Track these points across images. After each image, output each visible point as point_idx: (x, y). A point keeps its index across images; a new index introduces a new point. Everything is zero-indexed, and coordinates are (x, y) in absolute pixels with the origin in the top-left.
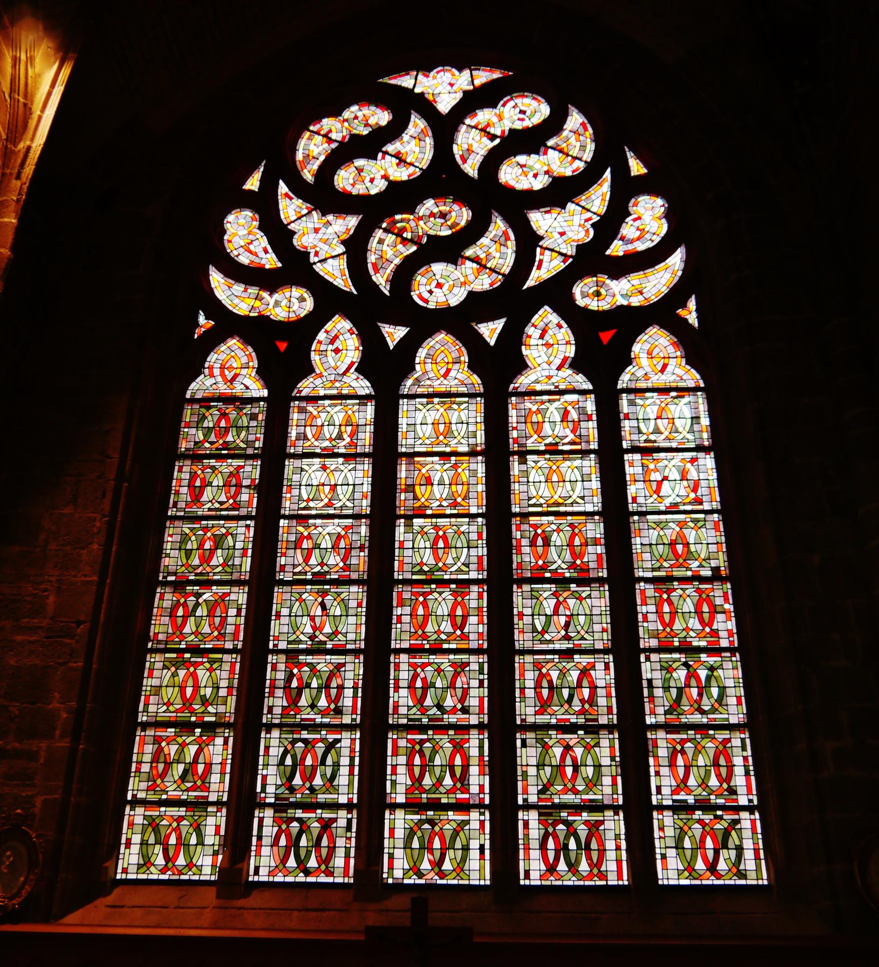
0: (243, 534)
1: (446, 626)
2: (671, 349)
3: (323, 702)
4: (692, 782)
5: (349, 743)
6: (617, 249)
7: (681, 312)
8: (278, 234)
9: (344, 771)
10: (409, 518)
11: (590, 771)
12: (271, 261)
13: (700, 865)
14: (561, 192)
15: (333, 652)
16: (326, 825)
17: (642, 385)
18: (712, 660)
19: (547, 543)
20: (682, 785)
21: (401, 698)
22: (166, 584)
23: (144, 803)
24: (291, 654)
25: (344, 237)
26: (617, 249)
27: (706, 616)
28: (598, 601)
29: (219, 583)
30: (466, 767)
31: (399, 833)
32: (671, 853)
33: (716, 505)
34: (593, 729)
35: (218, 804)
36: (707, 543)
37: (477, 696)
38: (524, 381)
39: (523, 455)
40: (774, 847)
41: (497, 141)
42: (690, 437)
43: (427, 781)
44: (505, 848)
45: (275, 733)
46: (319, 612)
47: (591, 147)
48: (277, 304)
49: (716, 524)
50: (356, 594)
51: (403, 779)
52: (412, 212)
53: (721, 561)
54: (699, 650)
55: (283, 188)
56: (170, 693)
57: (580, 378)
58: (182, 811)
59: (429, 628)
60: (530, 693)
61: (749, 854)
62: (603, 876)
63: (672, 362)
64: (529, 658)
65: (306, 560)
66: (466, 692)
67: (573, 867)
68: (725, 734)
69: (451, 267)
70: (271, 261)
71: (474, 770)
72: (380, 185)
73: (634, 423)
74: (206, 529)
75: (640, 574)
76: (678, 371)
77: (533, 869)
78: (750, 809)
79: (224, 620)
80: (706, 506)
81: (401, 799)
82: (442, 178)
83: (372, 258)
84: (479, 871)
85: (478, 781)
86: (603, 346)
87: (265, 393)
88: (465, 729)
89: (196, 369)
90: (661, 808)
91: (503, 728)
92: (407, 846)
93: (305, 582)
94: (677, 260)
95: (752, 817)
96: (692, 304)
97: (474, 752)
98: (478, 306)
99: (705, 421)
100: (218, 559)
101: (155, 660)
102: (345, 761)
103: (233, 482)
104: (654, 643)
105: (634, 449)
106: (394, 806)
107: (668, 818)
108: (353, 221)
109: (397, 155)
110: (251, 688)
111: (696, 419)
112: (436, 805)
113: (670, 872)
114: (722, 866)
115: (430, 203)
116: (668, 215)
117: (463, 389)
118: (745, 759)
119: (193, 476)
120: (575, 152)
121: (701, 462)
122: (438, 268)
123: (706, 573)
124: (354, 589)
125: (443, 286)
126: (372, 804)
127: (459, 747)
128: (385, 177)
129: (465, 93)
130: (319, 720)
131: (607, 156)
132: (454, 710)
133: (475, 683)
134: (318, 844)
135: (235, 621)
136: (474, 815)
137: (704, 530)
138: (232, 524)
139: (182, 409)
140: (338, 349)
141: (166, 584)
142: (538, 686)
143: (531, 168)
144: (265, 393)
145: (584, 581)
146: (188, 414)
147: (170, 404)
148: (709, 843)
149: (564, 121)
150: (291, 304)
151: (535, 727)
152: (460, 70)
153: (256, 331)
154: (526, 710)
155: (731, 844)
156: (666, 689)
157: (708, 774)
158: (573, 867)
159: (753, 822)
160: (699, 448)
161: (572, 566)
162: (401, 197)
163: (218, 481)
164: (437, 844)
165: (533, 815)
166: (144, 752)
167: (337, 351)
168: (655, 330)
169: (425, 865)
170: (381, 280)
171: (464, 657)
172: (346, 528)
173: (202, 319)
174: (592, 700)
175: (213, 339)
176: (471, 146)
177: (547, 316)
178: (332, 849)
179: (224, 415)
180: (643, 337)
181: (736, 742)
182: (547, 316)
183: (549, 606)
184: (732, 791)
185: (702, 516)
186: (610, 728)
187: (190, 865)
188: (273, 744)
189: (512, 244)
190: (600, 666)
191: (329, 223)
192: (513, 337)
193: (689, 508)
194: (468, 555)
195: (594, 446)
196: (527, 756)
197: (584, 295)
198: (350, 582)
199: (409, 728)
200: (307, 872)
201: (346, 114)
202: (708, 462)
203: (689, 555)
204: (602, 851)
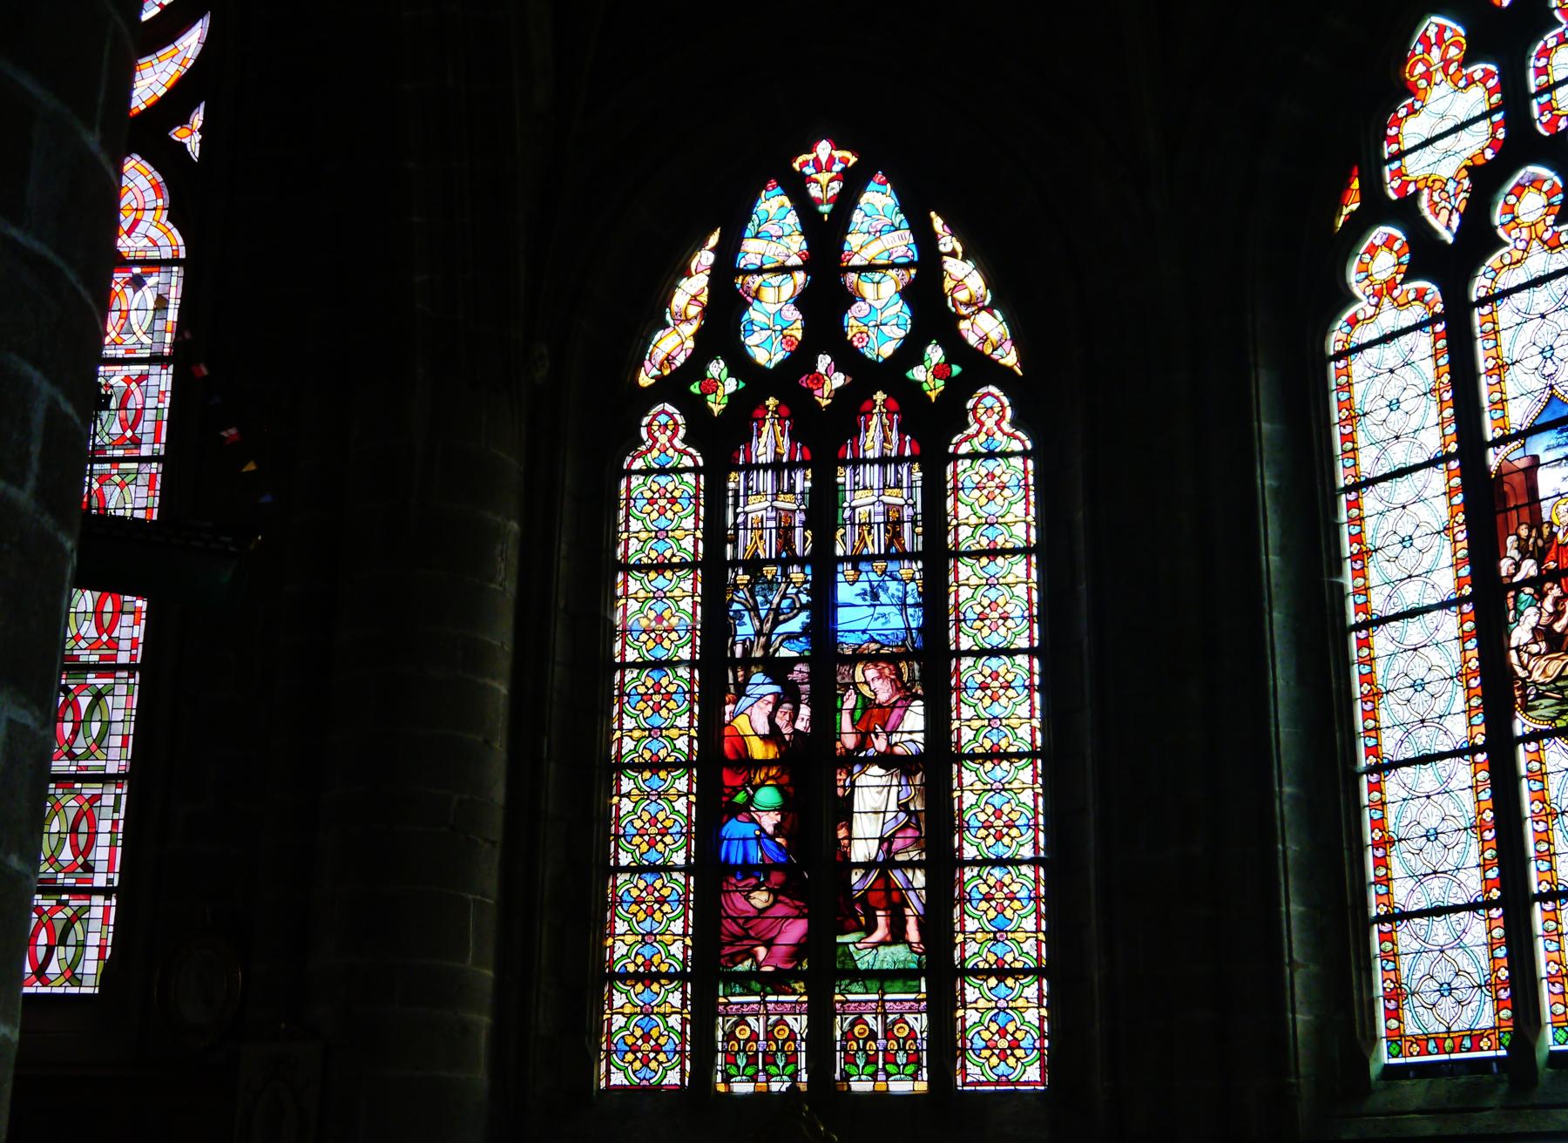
2: (150, 195)
18: (100, 682)
27: (107, 618)
33: (160, 449)
42: (146, 340)
49: (153, 477)
54: (88, 668)
63: (149, 216)
68: (95, 789)
76: (154, 233)
78: (106, 892)
80: (145, 451)
95: (108, 903)
96: (197, 119)
114: (54, 968)
118: (115, 823)
121: (153, 380)
137: (132, 487)
155: (71, 940)
157: (61, 842)
159: (107, 909)
160: (154, 360)
168: (133, 163)
181: (108, 800)
184: (89, 868)
185: (135, 465)
193: (119, 453)
202: (163, 379)
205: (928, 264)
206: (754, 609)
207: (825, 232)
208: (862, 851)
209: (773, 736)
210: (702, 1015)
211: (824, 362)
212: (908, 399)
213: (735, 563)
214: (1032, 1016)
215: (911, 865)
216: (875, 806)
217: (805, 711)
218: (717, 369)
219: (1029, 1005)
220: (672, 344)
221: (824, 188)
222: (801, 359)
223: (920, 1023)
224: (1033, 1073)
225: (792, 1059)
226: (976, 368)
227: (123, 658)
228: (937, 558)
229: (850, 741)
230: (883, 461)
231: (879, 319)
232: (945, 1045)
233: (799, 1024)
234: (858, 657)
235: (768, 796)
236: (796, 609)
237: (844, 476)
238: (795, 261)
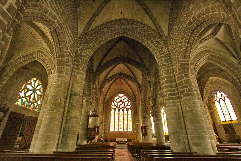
8: (114, 104)
14: (126, 102)
28: (127, 121)
36: (131, 119)
70: (114, 105)
82: (121, 101)
86: (127, 110)
125: (121, 107)
131: (128, 100)
140: (117, 109)
153: (114, 109)
162: (119, 102)
170: (119, 106)
177: (125, 108)
182: (125, 108)
192: (124, 109)
194: (122, 119)
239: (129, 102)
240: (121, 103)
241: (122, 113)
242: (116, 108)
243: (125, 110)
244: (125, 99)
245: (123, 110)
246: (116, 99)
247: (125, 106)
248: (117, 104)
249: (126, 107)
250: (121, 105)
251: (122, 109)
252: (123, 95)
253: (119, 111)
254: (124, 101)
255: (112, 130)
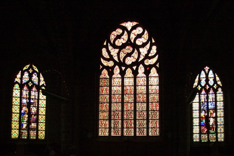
0: (108, 96)
1: (129, 108)
3: (117, 117)
4: (153, 125)
5: (120, 121)
6: (150, 55)
7: (157, 65)
8: (109, 52)
9: (120, 124)
10: (125, 94)
11: (143, 124)
12: (108, 57)
13: (153, 134)
14: (144, 45)
15: (118, 111)
16: (118, 130)
17: (151, 76)
18: (156, 112)
19: (140, 98)
20: (152, 126)
21: (125, 116)
22: (100, 103)
23: (101, 128)
24: (114, 111)
25: (117, 53)
26: (150, 55)
28: (145, 105)
29: (106, 103)
30: (131, 124)
31: (125, 131)
32: (150, 132)
34: (144, 120)
35: (108, 128)
36: (157, 97)
37: (133, 116)
38: (138, 75)
39: (138, 86)
40: (160, 132)
41: (136, 36)
43: (128, 125)
44: (135, 132)
45: (113, 120)
46: (116, 106)
47: (148, 37)
48: (109, 64)
50: (120, 104)
51: (125, 125)
52: (125, 48)
53: (158, 100)
55: (109, 44)
56: (102, 116)
57: (145, 75)
58: (104, 129)
59: (128, 108)
60: (138, 116)
61: (158, 133)
62: (144, 135)
63: (155, 73)
64: (138, 112)
65: (115, 100)
66: (131, 116)
67: (141, 134)
68: (156, 120)
69: (130, 58)
70: (108, 57)
71: (132, 124)
72: (121, 44)
73: (150, 81)
74: (104, 96)
75: (150, 101)
77: (138, 134)
78: (158, 128)
79: (107, 108)
80: (157, 93)
81: (125, 127)
82: (129, 43)
83: (120, 56)
84: (133, 134)
85: (133, 125)
87: (109, 77)
88: (131, 120)
89: (101, 74)
90: (150, 128)
91: (135, 119)
92: (126, 132)
93: (115, 103)
94: (157, 57)
96: (158, 64)
97: (132, 122)
98: (133, 64)
99: (158, 81)
100: (105, 100)
101: (100, 112)
102: (120, 123)
103: (106, 90)
104: (150, 110)
105: (150, 85)
106: (125, 128)
107: (150, 129)
108: (118, 50)
109: (123, 39)
110: (110, 115)
111: (157, 81)
112: (129, 128)
113: (150, 134)
114: (155, 134)
115: (127, 47)
116: (157, 49)
117: (131, 77)
119: (102, 89)
120: (146, 38)
122: (128, 58)
123: (157, 101)
124: (120, 103)
125: (129, 61)
126: (122, 128)
127: (131, 122)
128: (122, 42)
129: (132, 27)
130: (117, 119)
131: (150, 39)
132: (130, 118)
133: (132, 115)
134: (117, 132)
135: (108, 107)
136: (132, 129)
138: (106, 95)
139: (99, 80)
140: (117, 70)
141: (100, 103)
142: (139, 115)
143: (140, 41)
144: (109, 77)
145: (144, 102)
146: (100, 80)
147: (98, 79)
148: (154, 131)
149: (144, 33)
150: (111, 64)
151: (138, 119)
152: (131, 22)
153: (107, 68)
154: (137, 118)
156: (151, 115)
158: (141, 134)
160: (157, 85)
161: (143, 100)
162: (124, 46)
163: (105, 90)
164: (129, 132)
165: (138, 129)
166: (100, 122)
167: (117, 71)
169: (128, 134)
170: (122, 60)
171: (131, 112)
172: (119, 96)
173: (101, 66)
174: (144, 116)
175: (102, 69)
176: (133, 37)
177: (141, 66)
178: (119, 133)
179: (104, 81)
180: (152, 69)
182: (141, 66)
183: (140, 105)
184: (157, 126)
186: (145, 119)
187: (106, 134)
188: (113, 121)
189: (137, 54)
190: (145, 112)
191: (115, 51)
192: (137, 69)
194: (131, 100)
195: (146, 85)
196: (137, 123)
197: (146, 62)
198: (119, 103)
199: (126, 120)
200: (117, 135)
201: (116, 31)
202: (158, 87)
203: (155, 99)
204: (144, 133)
205: (215, 77)
206: (203, 106)
207: (207, 75)
208: (211, 124)
209: (204, 116)
210: (200, 136)
211: (207, 86)
212: (213, 89)
213: (201, 102)
214: (223, 136)
215: (214, 125)
216: (212, 121)
217: (207, 114)
218: (199, 86)
219: (223, 135)
220: (196, 84)
221: (207, 71)
222: (205, 85)
223: (215, 137)
224: (223, 140)
225: (206, 139)
226: (218, 86)
227: (158, 110)
228: (216, 101)
229: (210, 116)
230: (212, 94)
231: (211, 82)
232: (217, 138)
233: (207, 137)
234: (210, 109)
235: (204, 120)
236: (206, 106)
237: (209, 95)
238: (205, 77)
239: (152, 45)
240: (128, 49)
241: (132, 80)
242: (114, 66)
243: (139, 71)
244: (139, 36)
245: (135, 73)
246: (112, 37)
247: (140, 59)
248: (118, 54)
249: (142, 62)
250: (129, 55)
251: (132, 69)
252: (135, 23)
253: (123, 73)
254: (139, 42)
255: (103, 132)
